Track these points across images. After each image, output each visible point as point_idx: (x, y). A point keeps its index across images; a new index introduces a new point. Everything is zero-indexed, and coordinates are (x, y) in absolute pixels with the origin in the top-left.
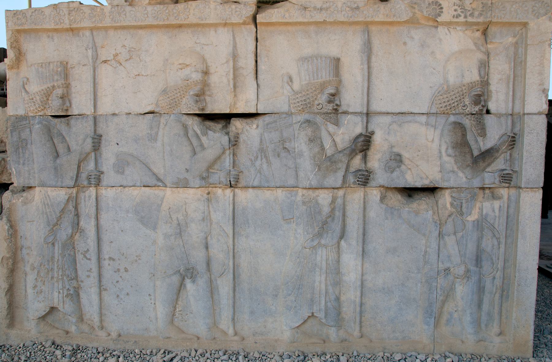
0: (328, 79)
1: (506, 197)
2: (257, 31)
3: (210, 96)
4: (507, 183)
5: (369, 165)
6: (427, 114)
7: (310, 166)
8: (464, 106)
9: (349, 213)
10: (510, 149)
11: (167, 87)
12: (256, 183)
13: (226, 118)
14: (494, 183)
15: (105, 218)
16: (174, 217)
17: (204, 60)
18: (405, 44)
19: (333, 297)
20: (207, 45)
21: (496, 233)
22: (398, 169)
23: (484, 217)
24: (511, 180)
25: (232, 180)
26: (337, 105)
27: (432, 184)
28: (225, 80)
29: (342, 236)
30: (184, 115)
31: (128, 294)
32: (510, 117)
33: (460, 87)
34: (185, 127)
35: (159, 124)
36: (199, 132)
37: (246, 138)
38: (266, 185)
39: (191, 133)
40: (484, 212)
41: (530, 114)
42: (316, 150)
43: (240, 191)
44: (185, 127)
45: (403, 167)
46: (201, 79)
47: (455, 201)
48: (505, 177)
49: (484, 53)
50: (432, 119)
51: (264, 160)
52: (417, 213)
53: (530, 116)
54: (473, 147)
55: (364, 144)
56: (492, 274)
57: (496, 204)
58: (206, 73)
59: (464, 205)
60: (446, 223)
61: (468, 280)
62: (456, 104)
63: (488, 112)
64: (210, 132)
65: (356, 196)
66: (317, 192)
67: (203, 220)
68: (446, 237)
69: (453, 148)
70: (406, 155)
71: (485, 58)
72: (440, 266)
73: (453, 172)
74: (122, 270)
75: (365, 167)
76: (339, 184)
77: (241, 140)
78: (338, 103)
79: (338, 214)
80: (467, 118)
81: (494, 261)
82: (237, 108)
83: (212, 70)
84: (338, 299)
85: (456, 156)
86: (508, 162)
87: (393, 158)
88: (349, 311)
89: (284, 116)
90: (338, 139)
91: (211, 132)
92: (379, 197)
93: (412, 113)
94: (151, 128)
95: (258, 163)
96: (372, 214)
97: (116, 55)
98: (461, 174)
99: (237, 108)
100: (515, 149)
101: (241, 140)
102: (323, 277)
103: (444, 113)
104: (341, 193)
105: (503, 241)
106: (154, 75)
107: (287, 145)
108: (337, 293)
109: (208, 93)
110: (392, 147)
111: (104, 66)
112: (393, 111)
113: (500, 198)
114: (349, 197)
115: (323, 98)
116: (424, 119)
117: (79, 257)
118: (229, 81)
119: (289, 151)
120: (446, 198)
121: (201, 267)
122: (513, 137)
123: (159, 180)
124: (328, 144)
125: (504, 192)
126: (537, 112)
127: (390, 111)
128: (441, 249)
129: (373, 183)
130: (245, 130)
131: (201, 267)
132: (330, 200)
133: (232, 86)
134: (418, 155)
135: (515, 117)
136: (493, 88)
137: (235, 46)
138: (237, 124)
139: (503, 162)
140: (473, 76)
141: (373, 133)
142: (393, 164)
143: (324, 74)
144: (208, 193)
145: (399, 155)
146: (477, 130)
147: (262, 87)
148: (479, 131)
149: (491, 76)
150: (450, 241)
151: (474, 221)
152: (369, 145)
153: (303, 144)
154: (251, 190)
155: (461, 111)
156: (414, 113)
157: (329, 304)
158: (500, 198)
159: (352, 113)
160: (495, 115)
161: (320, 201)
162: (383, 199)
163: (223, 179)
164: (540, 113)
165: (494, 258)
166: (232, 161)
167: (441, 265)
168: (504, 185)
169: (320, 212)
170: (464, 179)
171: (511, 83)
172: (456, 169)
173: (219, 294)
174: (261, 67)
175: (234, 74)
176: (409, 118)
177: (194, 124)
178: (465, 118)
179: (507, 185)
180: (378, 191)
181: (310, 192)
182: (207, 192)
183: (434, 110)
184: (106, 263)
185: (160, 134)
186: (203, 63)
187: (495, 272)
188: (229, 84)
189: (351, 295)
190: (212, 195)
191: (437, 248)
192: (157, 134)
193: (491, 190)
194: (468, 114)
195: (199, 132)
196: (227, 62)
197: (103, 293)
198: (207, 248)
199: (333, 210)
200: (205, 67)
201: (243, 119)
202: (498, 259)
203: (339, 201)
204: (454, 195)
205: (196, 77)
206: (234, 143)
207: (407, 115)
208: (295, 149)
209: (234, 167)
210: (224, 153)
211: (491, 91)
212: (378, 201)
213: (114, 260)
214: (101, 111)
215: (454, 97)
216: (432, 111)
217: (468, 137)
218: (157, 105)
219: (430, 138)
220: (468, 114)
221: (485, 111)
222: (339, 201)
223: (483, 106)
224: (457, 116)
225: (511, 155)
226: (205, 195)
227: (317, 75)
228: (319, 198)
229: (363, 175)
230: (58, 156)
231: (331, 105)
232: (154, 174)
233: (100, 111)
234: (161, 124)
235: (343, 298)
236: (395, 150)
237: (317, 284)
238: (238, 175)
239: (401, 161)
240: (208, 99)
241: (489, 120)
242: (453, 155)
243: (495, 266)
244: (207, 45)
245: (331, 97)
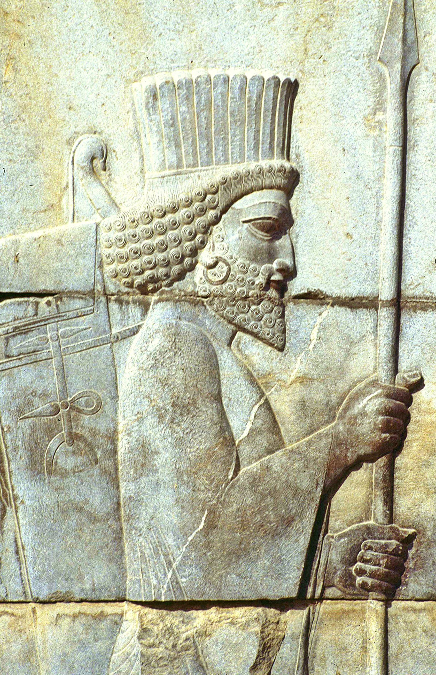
5: (403, 504)
7: (177, 510)
42: (203, 442)
66: (200, 617)
75: (391, 517)
76: (289, 588)
78: (288, 262)
89: (78, 304)
90: (284, 404)
104: (294, 619)
114: (325, 639)
115: (231, 240)
153: (151, 421)
161: (214, 656)
181: (173, 618)
208: (112, 437)
228: (207, 641)
229: (384, 549)
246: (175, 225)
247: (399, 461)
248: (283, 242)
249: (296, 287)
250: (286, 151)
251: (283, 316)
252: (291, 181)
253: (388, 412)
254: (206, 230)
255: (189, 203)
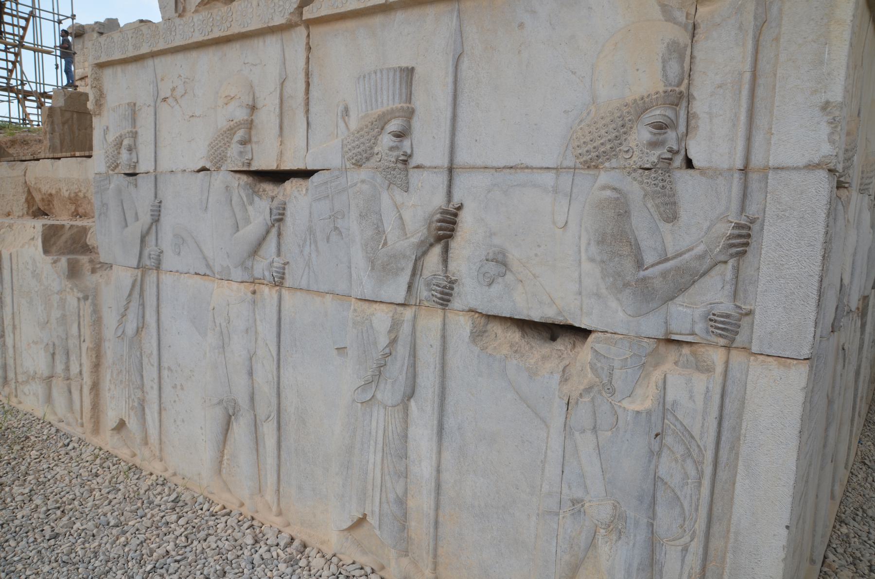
0: (391, 106)
1: (719, 369)
2: (308, 36)
3: (257, 142)
4: (721, 336)
5: (452, 266)
6: (556, 169)
8: (627, 151)
9: (422, 353)
10: (732, 256)
12: (304, 284)
13: (279, 177)
14: (693, 334)
15: (164, 311)
16: (217, 322)
18: (521, 25)
19: (392, 496)
21: (695, 452)
22: (500, 280)
23: (668, 406)
24: (737, 333)
25: (275, 274)
26: (405, 154)
27: (561, 319)
29: (411, 394)
31: (183, 421)
32: (577, 171)
33: (619, 109)
36: (245, 199)
38: (315, 288)
39: (235, 199)
40: (670, 398)
41: (782, 169)
45: (509, 277)
46: (246, 118)
47: (600, 361)
48: (715, 321)
49: (685, 27)
50: (566, 179)
51: (313, 246)
52: (532, 373)
53: (783, 174)
54: (643, 245)
55: (445, 228)
56: (682, 541)
57: (700, 382)
58: (253, 108)
59: (617, 373)
60: (577, 403)
61: (620, 538)
62: (608, 146)
63: (689, 164)
64: (256, 199)
65: (431, 322)
66: (376, 306)
67: (247, 331)
68: (577, 434)
69: (598, 243)
70: (514, 255)
71: (684, 38)
72: (563, 492)
73: (598, 295)
74: (179, 387)
79: (402, 351)
80: (635, 179)
81: (687, 513)
83: (259, 105)
84: (401, 502)
85: (603, 262)
86: (728, 287)
87: (491, 256)
88: (420, 529)
90: (407, 216)
92: (469, 331)
93: (527, 168)
95: (307, 250)
96: (455, 361)
97: (173, 89)
98: (613, 304)
100: (749, 256)
101: (288, 213)
102: (379, 455)
103: (588, 167)
104: (408, 313)
105: (708, 470)
107: (340, 223)
108: (400, 491)
109: (254, 139)
110: (492, 234)
111: (164, 104)
112: (495, 164)
113: (709, 370)
114: (421, 323)
116: (548, 178)
117: (145, 360)
119: (340, 233)
120: (585, 352)
121: (243, 401)
122: (738, 226)
123: (208, 266)
124: (390, 225)
125: (717, 357)
126: (802, 162)
127: (489, 163)
128: (567, 458)
129: (457, 303)
131: (243, 401)
132: (388, 324)
134: (536, 255)
135: (754, 177)
136: (699, 106)
138: (290, 185)
139: (719, 286)
140: (648, 81)
141: (460, 208)
142: (492, 268)
143: (385, 98)
144: (254, 292)
145: (503, 253)
146: (657, 206)
147: (313, 126)
148: (662, 209)
149: (697, 78)
150: (586, 443)
151: (638, 412)
152: (453, 230)
154: (299, 293)
155: (622, 162)
156: (532, 168)
157: (385, 506)
158: (709, 370)
159: (430, 167)
160: (703, 171)
162: (477, 335)
163: (267, 273)
164: (811, 167)
165: (686, 505)
167: (565, 490)
168: (715, 339)
169: (375, 343)
170: (621, 314)
171: (745, 92)
172: (604, 291)
173: (264, 447)
174: (314, 93)
176: (521, 176)
178: (629, 179)
179: (722, 342)
180: (467, 317)
181: (365, 305)
182: (251, 289)
183: (570, 162)
184: (165, 373)
187: (687, 538)
189: (421, 502)
190: (258, 295)
191: (561, 453)
193: (695, 348)
194: (635, 170)
197: (163, 413)
198: (251, 374)
199: (393, 342)
200: (251, 99)
202: (697, 510)
203: (406, 328)
204: (597, 347)
205: (241, 115)
206: (279, 218)
207: (518, 171)
209: (279, 254)
210: (268, 232)
211: (695, 115)
212: (467, 339)
213: (171, 370)
214: (165, 165)
215: (603, 132)
216: (567, 163)
217: (634, 221)
219: (560, 220)
220: (635, 170)
221: (679, 160)
222: (406, 328)
223: (670, 151)
224: (613, 173)
225: (737, 270)
226: (249, 294)
227: (376, 101)
230: (127, 226)
231: (395, 153)
232: (205, 258)
233: (159, 169)
235: (411, 503)
236: (496, 241)
237: (371, 466)
238: (284, 269)
239: (505, 264)
240: (254, 146)
241: (686, 184)
242: (598, 258)
243: (687, 523)
245: (394, 139)
246: (362, 136)
247: (454, 244)
248: (406, 143)
249: (413, 162)
250: (409, 99)
251: (407, 175)
252: (410, 114)
253: (440, 221)
254: (376, 138)
255: (367, 126)
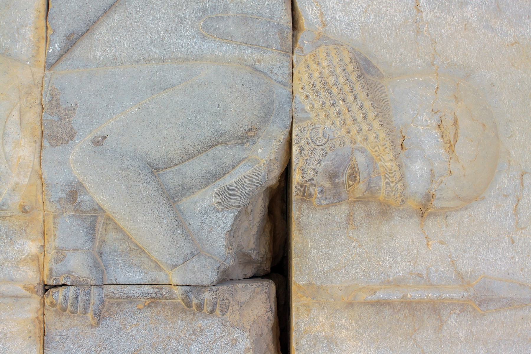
3: (350, 218)
11: (380, 76)
13: (276, 267)
17: (467, 201)
20: (516, 212)
28: (400, 270)
30: (286, 132)
34: (248, 136)
35: (256, 47)
36: (230, 180)
37: (210, 338)
39: (225, 154)
43: (32, 315)
44: (248, 136)
58: (425, 209)
77: (203, 323)
82: (308, 308)
83: (433, 226)
91: (230, 222)
94: (244, 19)
99: (308, 308)
106: (418, 32)
118: (398, 283)
123: (72, 41)
130: (235, 333)
133: (381, 294)
137: (511, 304)
166: (131, 291)
175: (419, 302)
177: (258, 165)
185: (226, 50)
186: (457, 197)
188: (387, 283)
192: (226, 37)
195: (230, 180)
196: (460, 277)
200: (444, 204)
201: (271, 324)
218: (321, 40)
232: (90, 27)
234: (257, 54)
244: (516, 212)
